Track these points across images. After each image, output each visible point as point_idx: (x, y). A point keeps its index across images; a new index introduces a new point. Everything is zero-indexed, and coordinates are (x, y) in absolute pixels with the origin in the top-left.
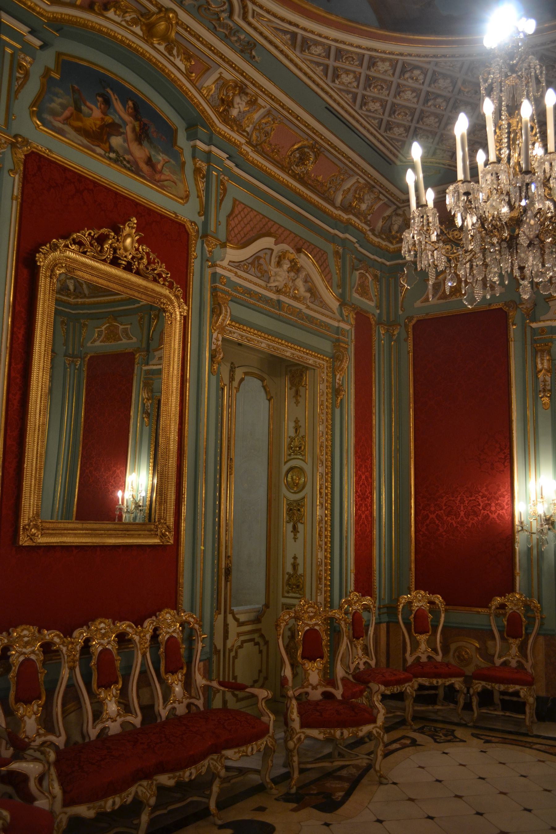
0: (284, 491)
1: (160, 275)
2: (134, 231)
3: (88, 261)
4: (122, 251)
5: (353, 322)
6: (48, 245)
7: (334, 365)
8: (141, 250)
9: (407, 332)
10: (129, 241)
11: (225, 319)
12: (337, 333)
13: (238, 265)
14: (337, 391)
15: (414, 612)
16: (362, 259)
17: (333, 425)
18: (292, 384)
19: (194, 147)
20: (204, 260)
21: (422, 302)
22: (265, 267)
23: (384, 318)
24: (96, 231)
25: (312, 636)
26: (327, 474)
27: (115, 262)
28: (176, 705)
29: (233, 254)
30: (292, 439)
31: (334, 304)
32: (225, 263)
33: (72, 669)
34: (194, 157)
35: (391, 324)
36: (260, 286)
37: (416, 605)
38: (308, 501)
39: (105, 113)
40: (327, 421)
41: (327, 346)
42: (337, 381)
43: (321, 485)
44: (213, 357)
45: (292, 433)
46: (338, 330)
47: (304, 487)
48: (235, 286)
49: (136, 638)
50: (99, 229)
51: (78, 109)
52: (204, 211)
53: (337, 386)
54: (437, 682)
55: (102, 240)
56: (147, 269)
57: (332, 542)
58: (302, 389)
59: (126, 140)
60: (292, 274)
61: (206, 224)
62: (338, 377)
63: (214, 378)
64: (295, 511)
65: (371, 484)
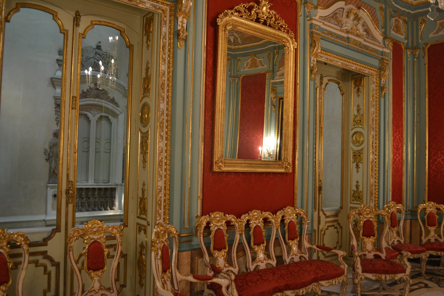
0: (351, 145)
1: (282, 27)
2: (267, 2)
4: (261, 14)
5: (391, 48)
6: (223, 14)
7: (380, 73)
8: (271, 13)
9: (424, 53)
10: (264, 8)
12: (382, 55)
14: (382, 89)
15: (427, 214)
16: (396, 11)
17: (380, 108)
18: (356, 85)
20: (305, 16)
21: (434, 34)
22: (339, 19)
23: (410, 45)
24: (247, 4)
25: (368, 224)
26: (376, 135)
27: (257, 21)
28: (294, 256)
29: (321, 12)
30: (356, 116)
31: (380, 38)
32: (317, 18)
33: (241, 235)
35: (414, 48)
37: (428, 210)
38: (365, 151)
40: (376, 105)
41: (376, 63)
42: (382, 82)
43: (372, 142)
44: (311, 71)
45: (356, 113)
46: (382, 53)
47: (362, 143)
48: (323, 31)
49: (273, 221)
50: (249, 3)
53: (382, 85)
54: (441, 254)
55: (250, 9)
56: (275, 23)
57: (379, 174)
60: (355, 22)
62: (382, 80)
63: (312, 83)
64: (358, 156)
65: (402, 141)
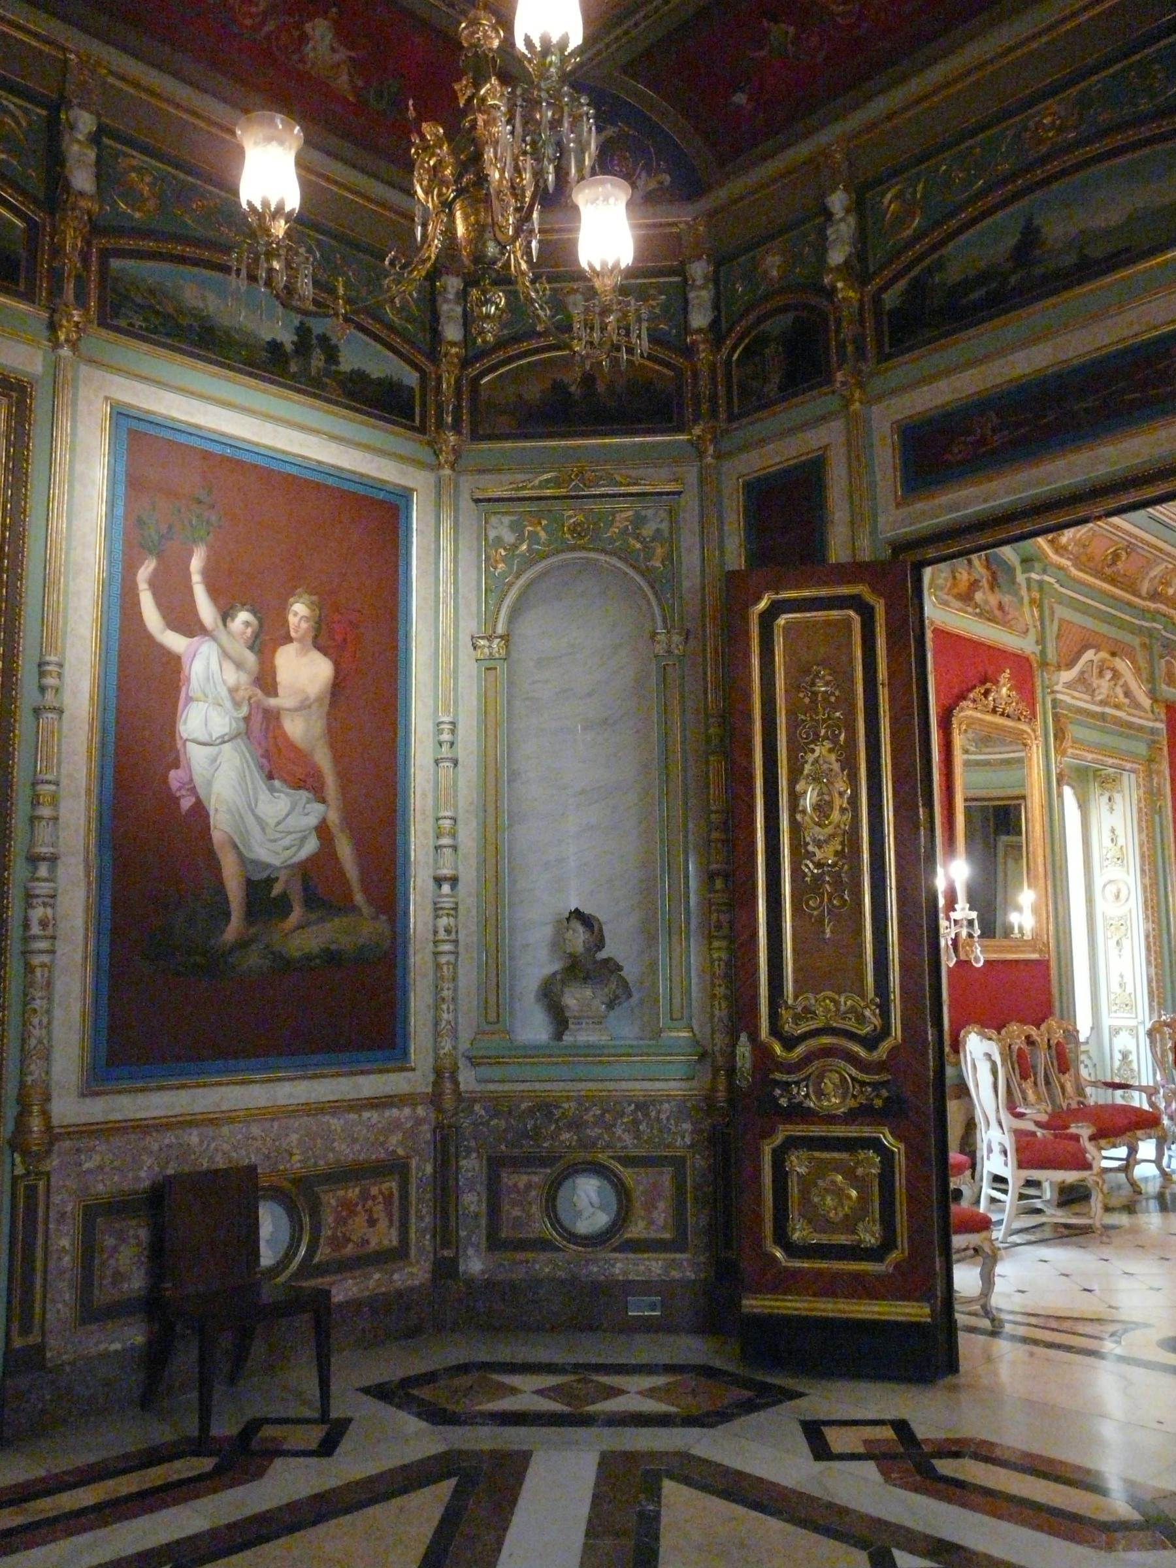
3: (979, 715)
10: (1004, 690)
11: (1067, 743)
13: (1069, 685)
19: (1028, 580)
27: (994, 711)
29: (1067, 676)
31: (1146, 702)
32: (1061, 685)
34: (1029, 589)
36: (1087, 702)
39: (969, 574)
45: (1107, 842)
46: (1153, 731)
51: (954, 578)
52: (1041, 641)
55: (986, 693)
58: (1117, 797)
59: (984, 593)
61: (1043, 652)
